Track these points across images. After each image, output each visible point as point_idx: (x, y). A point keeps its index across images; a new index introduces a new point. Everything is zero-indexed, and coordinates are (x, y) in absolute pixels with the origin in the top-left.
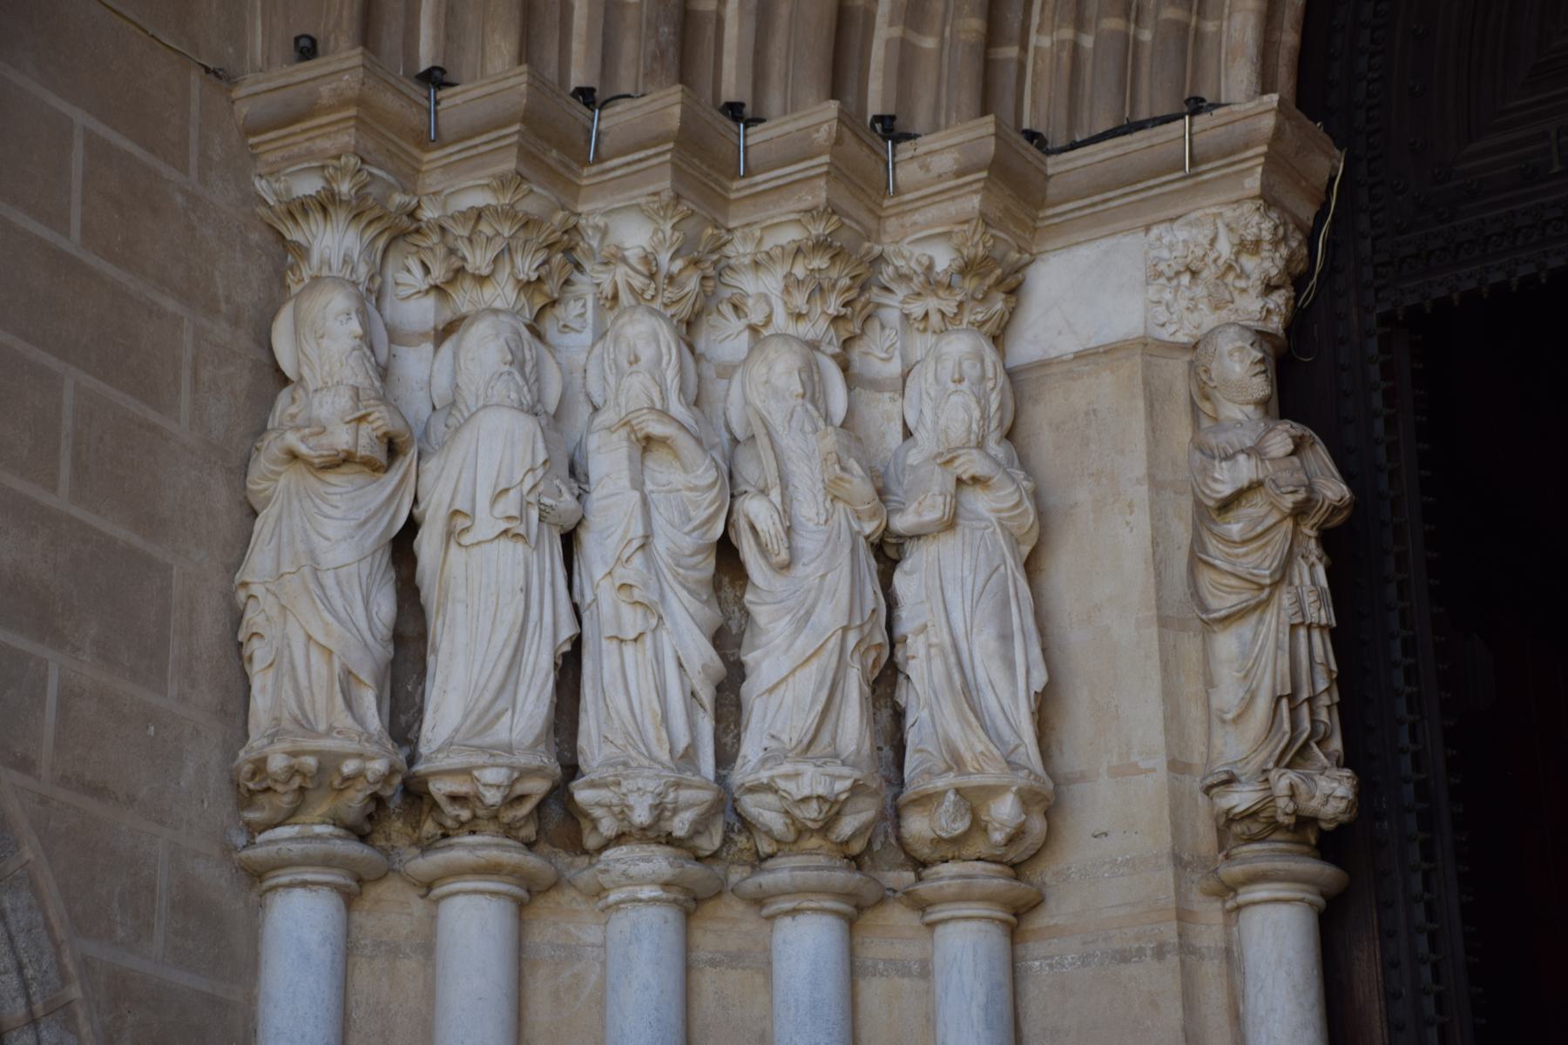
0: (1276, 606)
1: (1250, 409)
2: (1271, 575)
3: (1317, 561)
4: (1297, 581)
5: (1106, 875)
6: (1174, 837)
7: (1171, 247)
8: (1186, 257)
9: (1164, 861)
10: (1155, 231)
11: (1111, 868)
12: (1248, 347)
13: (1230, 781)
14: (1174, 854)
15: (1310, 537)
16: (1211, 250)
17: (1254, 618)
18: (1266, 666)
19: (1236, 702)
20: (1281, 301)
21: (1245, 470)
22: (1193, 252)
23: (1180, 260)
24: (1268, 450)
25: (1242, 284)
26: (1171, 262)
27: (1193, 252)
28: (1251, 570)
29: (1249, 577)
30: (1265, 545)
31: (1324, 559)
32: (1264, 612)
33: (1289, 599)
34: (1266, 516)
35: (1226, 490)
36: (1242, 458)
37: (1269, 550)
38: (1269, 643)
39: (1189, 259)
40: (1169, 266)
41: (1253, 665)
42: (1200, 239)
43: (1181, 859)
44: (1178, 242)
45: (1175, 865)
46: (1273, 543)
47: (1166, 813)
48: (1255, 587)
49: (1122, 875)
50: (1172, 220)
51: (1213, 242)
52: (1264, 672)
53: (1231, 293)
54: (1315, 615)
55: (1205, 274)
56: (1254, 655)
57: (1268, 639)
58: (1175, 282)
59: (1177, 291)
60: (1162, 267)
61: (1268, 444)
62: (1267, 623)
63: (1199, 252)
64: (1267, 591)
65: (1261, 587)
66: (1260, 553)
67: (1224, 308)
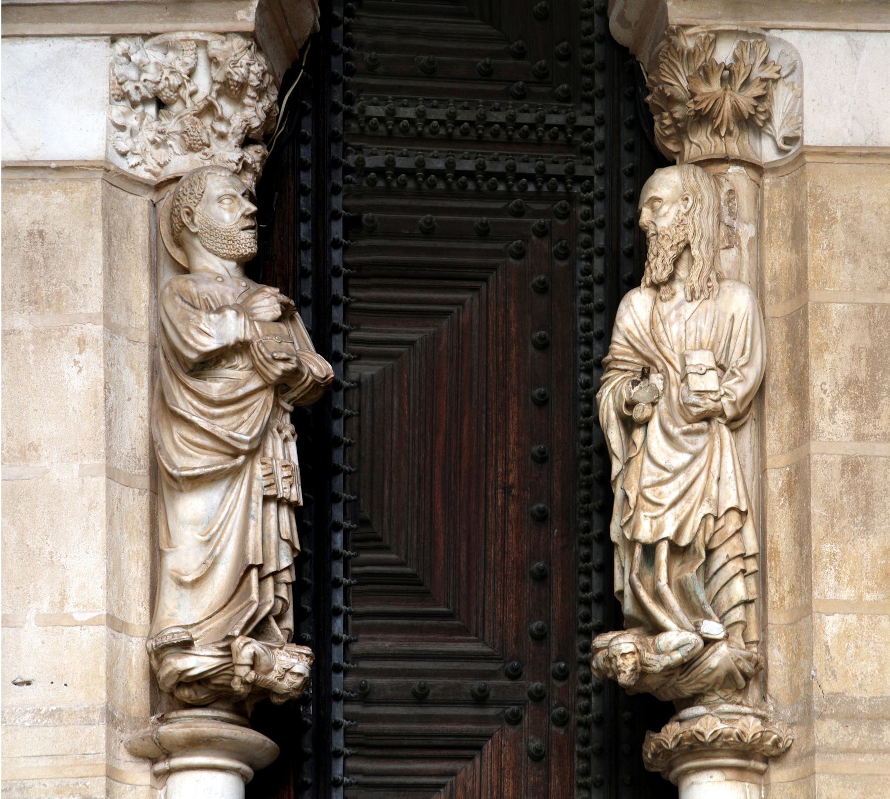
0: (247, 475)
1: (233, 264)
2: (250, 442)
3: (290, 437)
4: (270, 453)
5: (27, 724)
6: (108, 693)
7: (141, 68)
8: (158, 83)
9: (96, 717)
10: (122, 45)
11: (34, 718)
12: (240, 196)
13: (186, 645)
14: (107, 710)
15: (285, 411)
16: (188, 81)
17: (223, 485)
18: (231, 534)
19: (195, 566)
20: (257, 157)
21: (233, 328)
22: (167, 79)
23: (150, 85)
24: (255, 311)
25: (221, 127)
26: (139, 85)
27: (167, 79)
28: (232, 433)
29: (228, 440)
30: (243, 410)
31: (296, 436)
32: (234, 478)
33: (262, 469)
34: (248, 381)
35: (211, 344)
36: (230, 314)
37: (245, 416)
38: (236, 511)
39: (161, 86)
40: (137, 88)
41: (218, 530)
42: (178, 65)
43: (113, 717)
44: (149, 63)
45: (108, 722)
46: (250, 410)
47: (102, 669)
48: (230, 451)
49: (46, 725)
50: (146, 37)
51: (191, 74)
52: (228, 540)
53: (208, 135)
54: (287, 490)
55: (177, 107)
56: (220, 521)
57: (235, 507)
58: (140, 109)
59: (143, 119)
60: (129, 87)
61: (254, 305)
62: (235, 491)
63: (175, 81)
64: (242, 458)
65: (236, 454)
66: (235, 418)
67: (200, 150)
